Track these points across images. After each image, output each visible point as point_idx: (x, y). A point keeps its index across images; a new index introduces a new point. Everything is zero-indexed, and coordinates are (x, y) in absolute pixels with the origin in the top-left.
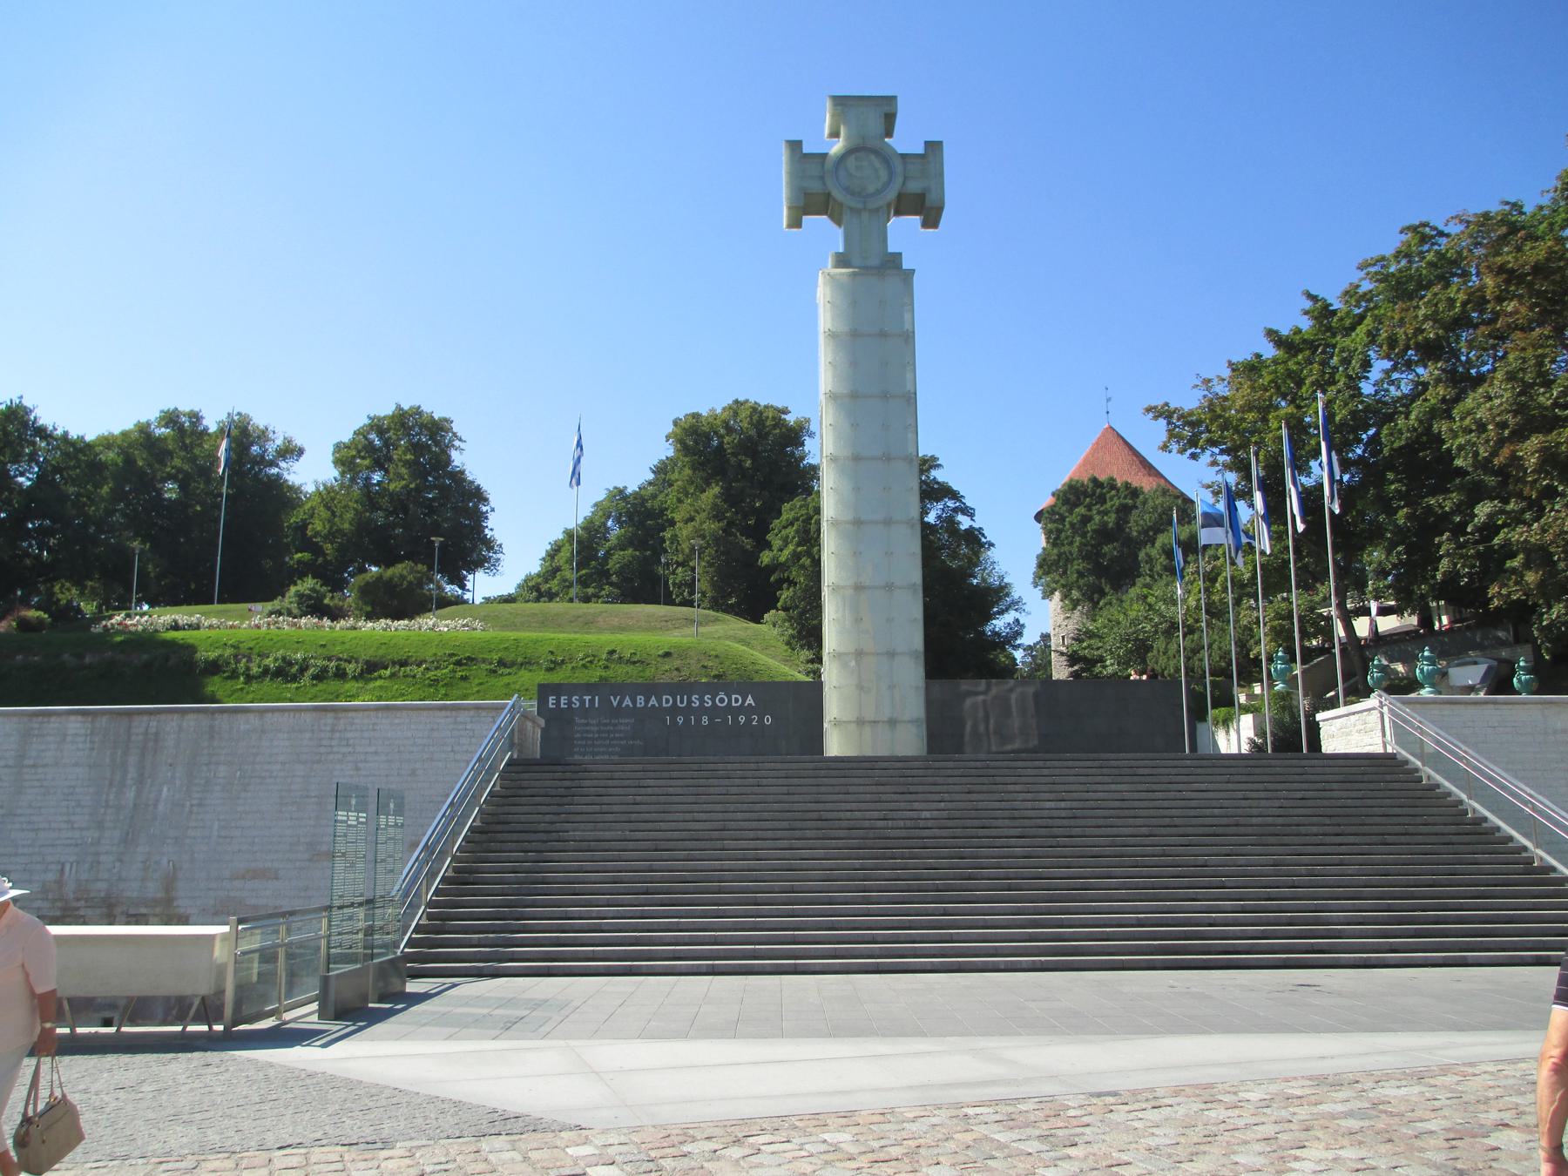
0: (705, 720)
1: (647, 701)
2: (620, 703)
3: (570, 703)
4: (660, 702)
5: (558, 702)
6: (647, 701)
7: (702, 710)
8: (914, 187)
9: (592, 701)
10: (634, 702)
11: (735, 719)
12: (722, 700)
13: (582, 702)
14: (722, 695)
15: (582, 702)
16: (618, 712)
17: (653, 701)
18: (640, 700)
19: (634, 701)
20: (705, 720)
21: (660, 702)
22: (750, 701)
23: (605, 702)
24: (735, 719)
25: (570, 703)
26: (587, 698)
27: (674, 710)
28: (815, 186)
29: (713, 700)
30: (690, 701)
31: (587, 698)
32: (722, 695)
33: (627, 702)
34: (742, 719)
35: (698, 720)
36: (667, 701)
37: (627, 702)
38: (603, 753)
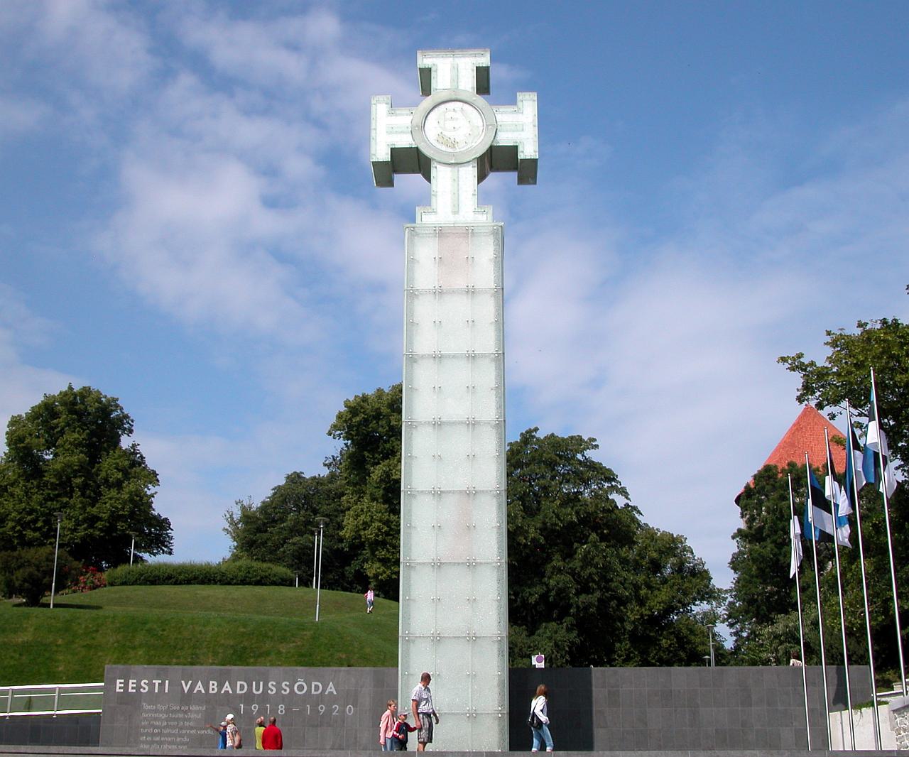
0: (281, 708)
1: (221, 686)
3: (139, 687)
4: (234, 689)
5: (126, 684)
6: (221, 686)
7: (280, 698)
9: (162, 685)
10: (207, 689)
11: (314, 709)
12: (300, 688)
13: (151, 685)
14: (301, 682)
15: (151, 685)
16: (187, 698)
17: (227, 687)
18: (213, 686)
19: (206, 687)
20: (281, 708)
21: (233, 686)
22: (331, 688)
24: (314, 709)
25: (139, 687)
26: (157, 682)
27: (249, 698)
29: (291, 687)
31: (157, 682)
32: (301, 682)
33: (200, 687)
34: (322, 709)
36: (241, 687)
38: (170, 743)
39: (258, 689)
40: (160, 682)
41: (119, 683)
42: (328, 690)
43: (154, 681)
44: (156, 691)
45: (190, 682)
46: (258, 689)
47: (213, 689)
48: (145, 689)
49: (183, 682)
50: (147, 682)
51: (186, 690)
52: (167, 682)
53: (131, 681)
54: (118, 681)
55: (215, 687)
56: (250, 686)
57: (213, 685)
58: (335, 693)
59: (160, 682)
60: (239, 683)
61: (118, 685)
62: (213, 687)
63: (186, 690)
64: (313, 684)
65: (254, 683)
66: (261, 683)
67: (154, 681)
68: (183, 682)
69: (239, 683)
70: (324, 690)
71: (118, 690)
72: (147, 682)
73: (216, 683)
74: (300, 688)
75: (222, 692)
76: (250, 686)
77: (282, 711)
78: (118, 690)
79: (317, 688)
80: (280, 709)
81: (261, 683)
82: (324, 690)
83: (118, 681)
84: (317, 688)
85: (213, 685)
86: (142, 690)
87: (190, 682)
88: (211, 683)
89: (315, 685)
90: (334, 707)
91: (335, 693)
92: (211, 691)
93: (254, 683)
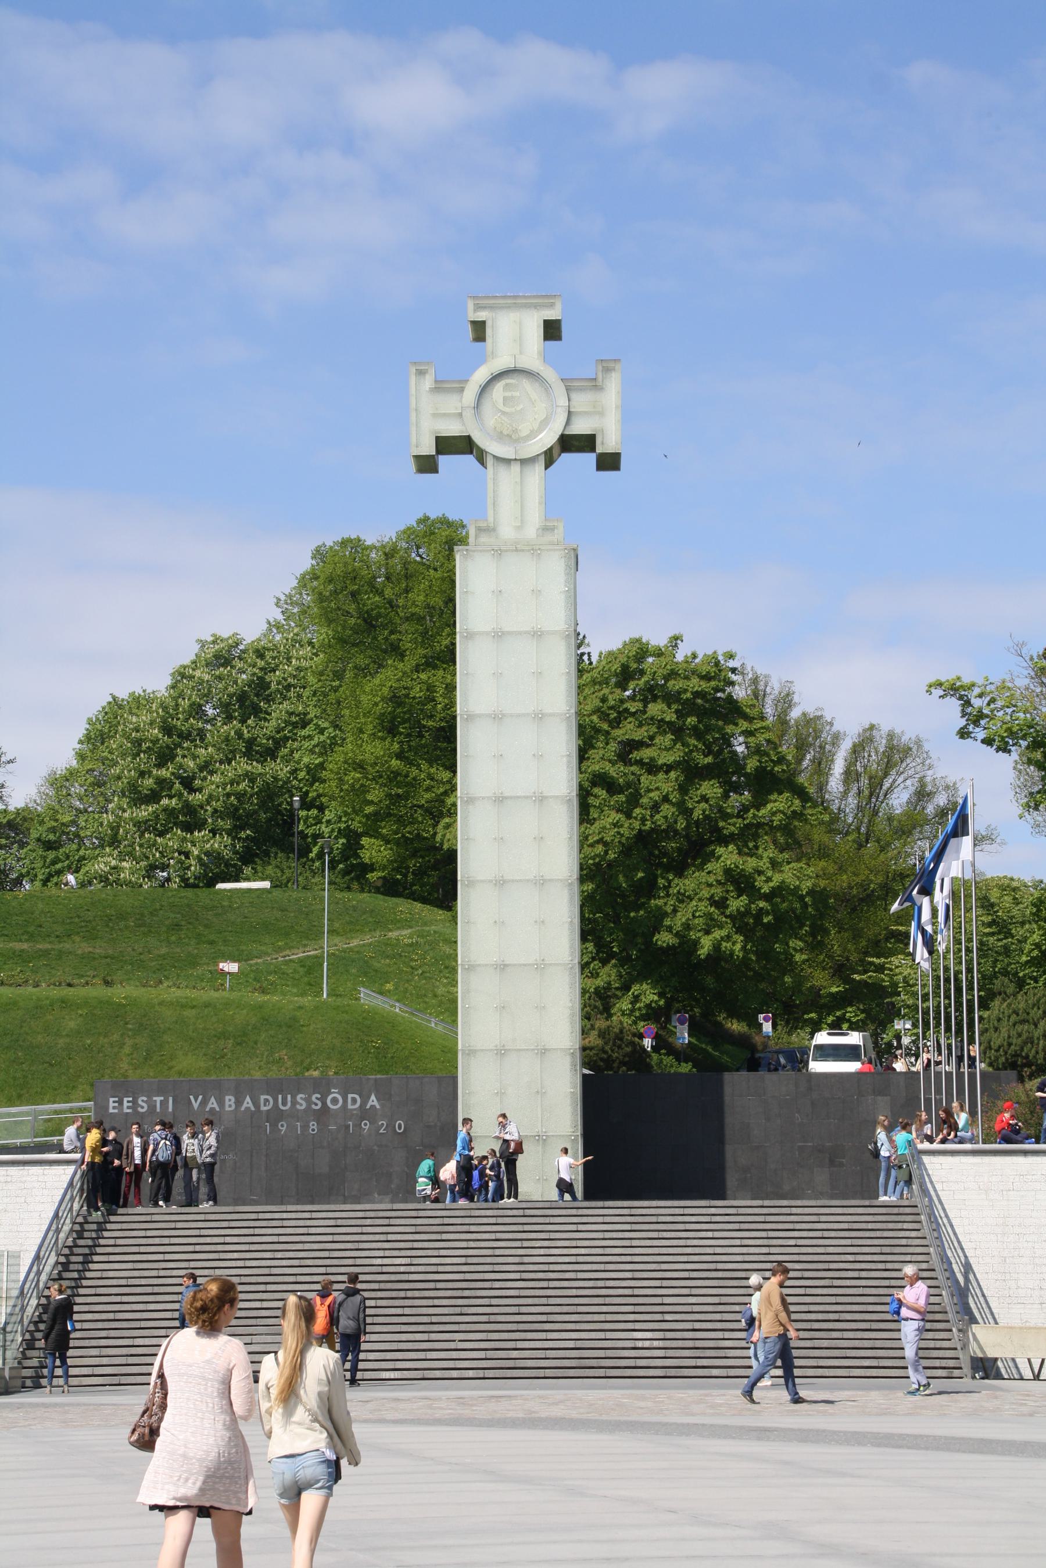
1: (239, 1102)
2: (204, 1102)
5: (121, 1102)
6: (239, 1102)
8: (580, 427)
10: (221, 1103)
12: (335, 1101)
17: (248, 1103)
18: (230, 1101)
22: (373, 1101)
23: (182, 1102)
26: (158, 1099)
28: (453, 429)
30: (294, 1103)
33: (213, 1103)
35: (306, 1127)
37: (213, 1103)
39: (284, 1104)
41: (112, 1102)
42: (370, 1103)
44: (158, 1110)
46: (284, 1104)
49: (192, 1097)
50: (145, 1099)
52: (171, 1099)
53: (126, 1100)
54: (112, 1100)
55: (232, 1102)
56: (276, 1100)
58: (378, 1107)
60: (263, 1097)
61: (111, 1105)
63: (196, 1105)
64: (350, 1096)
65: (280, 1097)
66: (289, 1096)
68: (192, 1097)
69: (263, 1097)
70: (364, 1102)
71: (111, 1111)
73: (233, 1099)
74: (335, 1101)
75: (243, 1109)
76: (276, 1100)
77: (313, 1130)
78: (111, 1111)
79: (354, 1101)
81: (289, 1096)
84: (354, 1101)
88: (227, 1098)
91: (378, 1107)
92: (227, 1109)
93: (280, 1097)
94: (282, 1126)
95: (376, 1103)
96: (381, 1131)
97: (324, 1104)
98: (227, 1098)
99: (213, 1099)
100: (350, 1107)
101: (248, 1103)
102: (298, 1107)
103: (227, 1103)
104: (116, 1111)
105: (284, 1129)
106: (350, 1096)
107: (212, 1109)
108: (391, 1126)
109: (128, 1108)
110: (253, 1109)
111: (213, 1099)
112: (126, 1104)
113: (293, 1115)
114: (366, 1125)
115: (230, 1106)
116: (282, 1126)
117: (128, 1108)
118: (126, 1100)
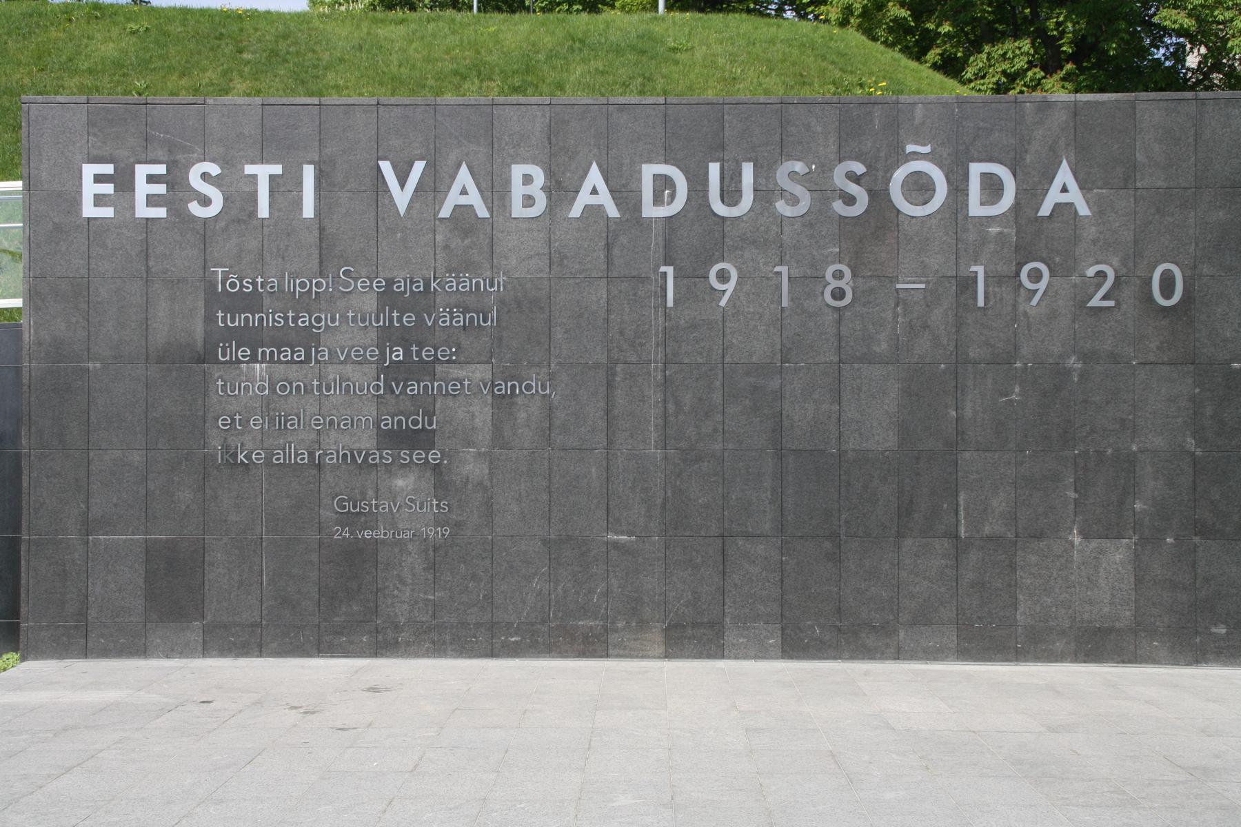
1: (561, 189)
2: (433, 188)
5: (123, 181)
6: (561, 189)
18: (527, 182)
26: (263, 172)
37: (464, 192)
39: (730, 194)
40: (277, 169)
42: (1054, 197)
43: (249, 169)
44: (263, 211)
45: (419, 166)
46: (730, 194)
47: (529, 201)
48: (210, 204)
49: (386, 166)
50: (214, 169)
51: (402, 198)
53: (142, 171)
54: (89, 170)
57: (527, 179)
59: (277, 169)
60: (649, 171)
61: (90, 189)
62: (528, 190)
63: (402, 198)
64: (977, 169)
65: (714, 169)
66: (748, 170)
67: (249, 169)
70: (1031, 193)
71: (89, 210)
72: (214, 169)
74: (920, 187)
75: (576, 211)
77: (839, 294)
78: (89, 210)
79: (992, 187)
80: (835, 284)
81: (748, 170)
82: (1031, 193)
83: (89, 170)
85: (527, 179)
86: (195, 209)
87: (419, 166)
88: (518, 171)
89: (983, 175)
90: (1091, 272)
92: (518, 210)
93: (714, 169)
94: (723, 276)
95: (1075, 196)
96: (1095, 302)
97: (879, 196)
98: (518, 171)
99: (464, 176)
100: (976, 209)
101: (594, 191)
102: (782, 207)
103: (518, 190)
104: (108, 212)
105: (730, 287)
106: (977, 169)
107: (463, 211)
108: (1131, 281)
109: (152, 201)
110: (613, 211)
111: (464, 176)
112: (142, 189)
113: (759, 236)
114: (1038, 281)
115: (529, 201)
116: (723, 276)
117: (152, 201)
118: (142, 171)
